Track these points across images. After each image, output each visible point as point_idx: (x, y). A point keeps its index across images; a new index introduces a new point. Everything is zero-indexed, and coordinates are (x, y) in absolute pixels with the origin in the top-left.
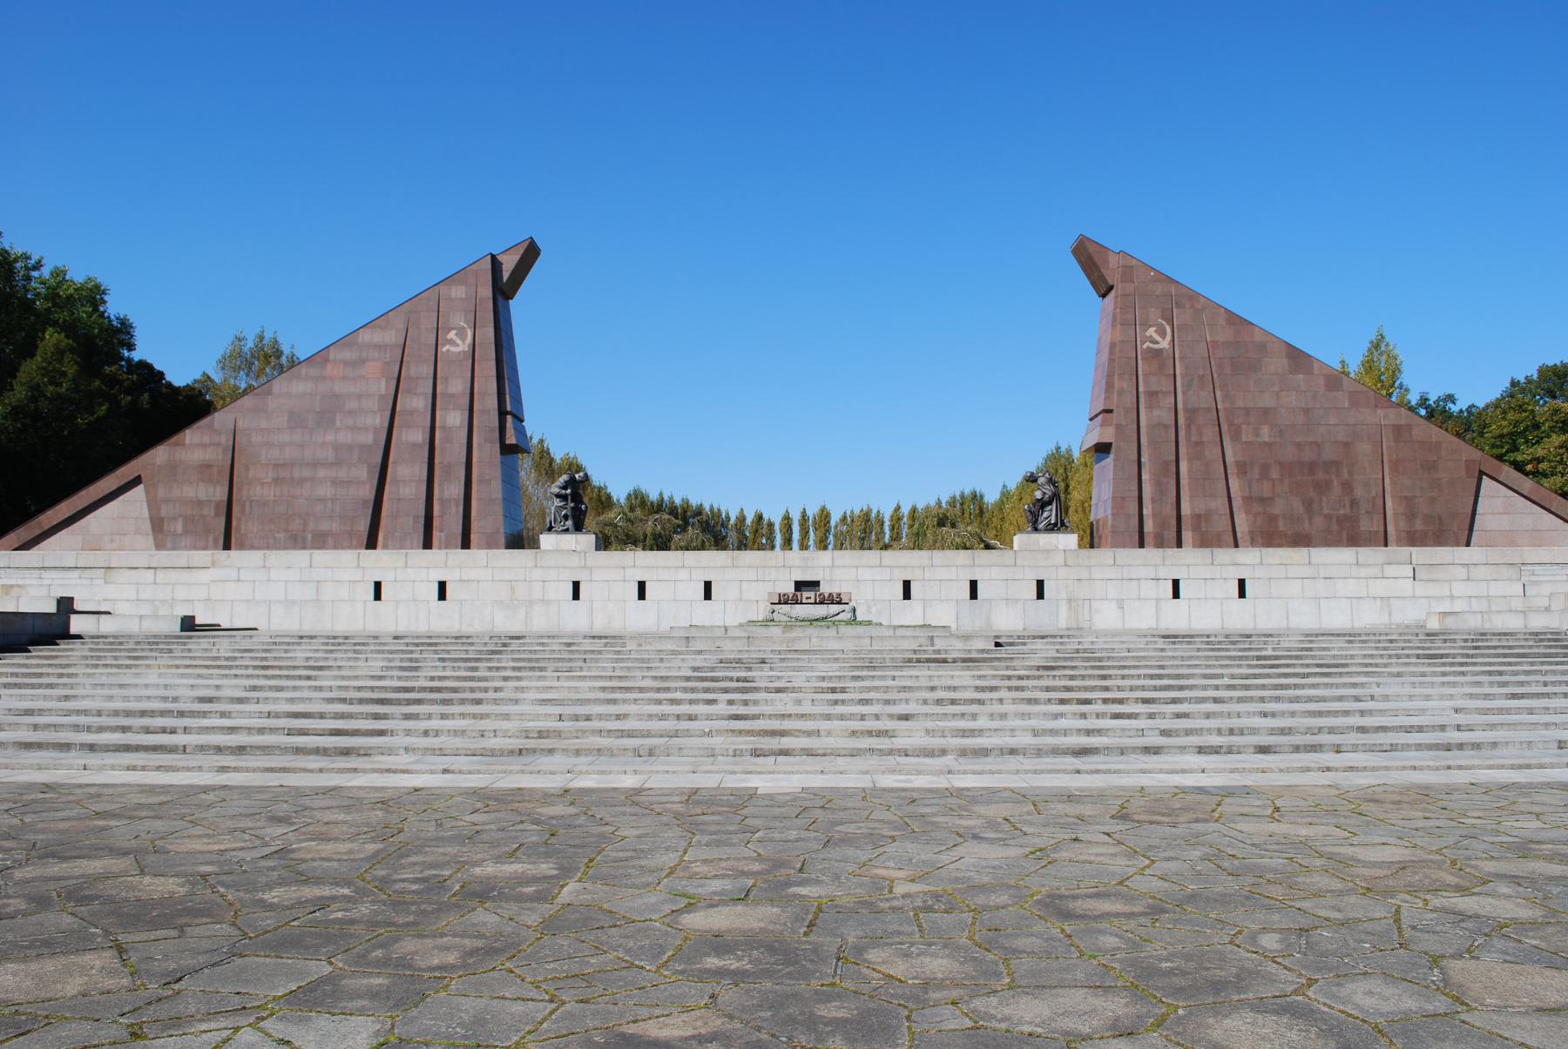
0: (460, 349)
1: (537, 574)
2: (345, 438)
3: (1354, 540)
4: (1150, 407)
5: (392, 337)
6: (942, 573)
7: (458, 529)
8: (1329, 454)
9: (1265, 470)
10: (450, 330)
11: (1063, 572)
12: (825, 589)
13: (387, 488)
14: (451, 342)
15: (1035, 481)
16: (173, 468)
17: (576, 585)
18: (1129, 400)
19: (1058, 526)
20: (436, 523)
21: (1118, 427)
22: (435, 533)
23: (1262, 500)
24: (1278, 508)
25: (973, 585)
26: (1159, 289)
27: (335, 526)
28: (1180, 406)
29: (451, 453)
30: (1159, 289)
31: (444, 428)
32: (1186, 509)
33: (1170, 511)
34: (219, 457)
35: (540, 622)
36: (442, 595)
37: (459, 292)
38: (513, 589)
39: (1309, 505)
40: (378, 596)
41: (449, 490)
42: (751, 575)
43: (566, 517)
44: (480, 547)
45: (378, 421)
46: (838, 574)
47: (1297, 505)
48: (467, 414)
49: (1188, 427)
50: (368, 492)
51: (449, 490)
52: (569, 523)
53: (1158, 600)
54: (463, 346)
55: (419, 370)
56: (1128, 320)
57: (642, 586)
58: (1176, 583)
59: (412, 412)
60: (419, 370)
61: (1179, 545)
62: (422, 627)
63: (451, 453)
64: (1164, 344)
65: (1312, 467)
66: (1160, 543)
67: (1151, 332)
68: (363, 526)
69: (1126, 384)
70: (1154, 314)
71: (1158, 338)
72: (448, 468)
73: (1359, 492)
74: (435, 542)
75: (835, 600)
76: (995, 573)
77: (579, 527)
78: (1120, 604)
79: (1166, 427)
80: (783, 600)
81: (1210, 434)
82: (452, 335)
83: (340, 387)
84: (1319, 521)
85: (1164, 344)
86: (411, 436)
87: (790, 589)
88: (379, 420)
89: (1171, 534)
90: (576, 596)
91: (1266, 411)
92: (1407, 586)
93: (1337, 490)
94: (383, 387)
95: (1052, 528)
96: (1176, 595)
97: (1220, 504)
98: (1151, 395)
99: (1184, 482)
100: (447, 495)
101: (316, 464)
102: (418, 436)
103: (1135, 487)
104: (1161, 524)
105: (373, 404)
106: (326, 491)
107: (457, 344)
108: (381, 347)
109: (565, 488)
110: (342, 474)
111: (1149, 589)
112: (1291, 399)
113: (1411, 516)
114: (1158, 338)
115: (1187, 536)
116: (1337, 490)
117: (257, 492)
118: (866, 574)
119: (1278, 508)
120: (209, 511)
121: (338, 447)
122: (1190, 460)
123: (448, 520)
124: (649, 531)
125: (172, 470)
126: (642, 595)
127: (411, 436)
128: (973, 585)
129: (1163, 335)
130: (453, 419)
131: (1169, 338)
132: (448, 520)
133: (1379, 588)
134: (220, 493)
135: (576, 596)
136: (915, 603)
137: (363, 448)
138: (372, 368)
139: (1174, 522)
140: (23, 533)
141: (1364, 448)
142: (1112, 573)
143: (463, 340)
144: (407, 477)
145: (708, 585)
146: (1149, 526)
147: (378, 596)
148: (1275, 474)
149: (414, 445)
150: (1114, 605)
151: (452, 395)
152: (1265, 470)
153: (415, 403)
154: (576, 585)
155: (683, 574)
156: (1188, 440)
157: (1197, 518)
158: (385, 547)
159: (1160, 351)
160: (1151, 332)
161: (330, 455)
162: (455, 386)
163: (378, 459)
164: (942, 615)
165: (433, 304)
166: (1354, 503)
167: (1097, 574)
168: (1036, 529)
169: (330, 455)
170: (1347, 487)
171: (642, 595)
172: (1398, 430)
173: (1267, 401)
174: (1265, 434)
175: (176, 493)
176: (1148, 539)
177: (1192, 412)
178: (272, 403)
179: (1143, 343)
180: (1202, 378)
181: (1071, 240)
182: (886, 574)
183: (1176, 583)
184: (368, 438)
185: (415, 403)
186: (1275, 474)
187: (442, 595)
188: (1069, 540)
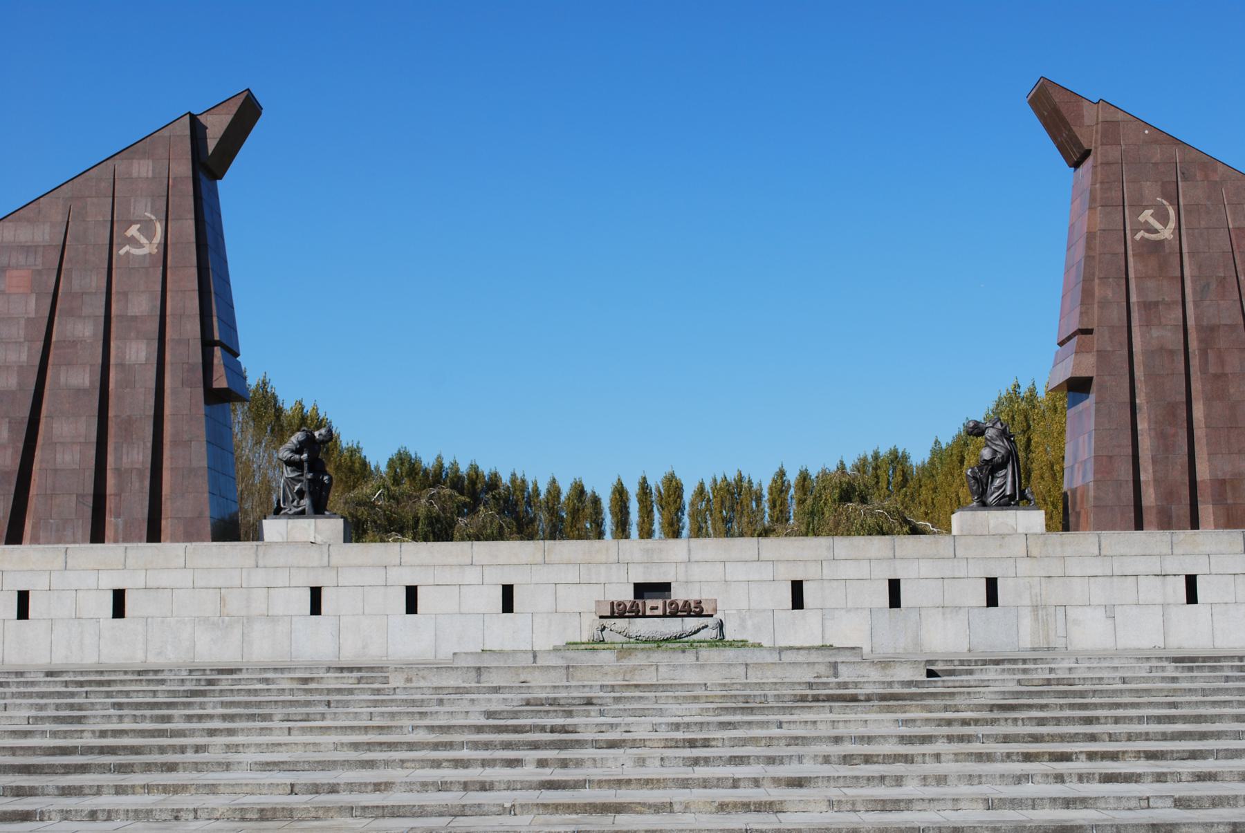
0: (145, 251)
1: (259, 578)
4: (1147, 324)
5: (44, 234)
6: (849, 570)
7: (142, 511)
10: (131, 223)
11: (1025, 567)
12: (679, 594)
13: (38, 453)
14: (133, 241)
15: (982, 433)
17: (316, 593)
18: (1116, 315)
20: (110, 504)
21: (1102, 355)
22: (110, 520)
25: (894, 587)
26: (1157, 154)
28: (1191, 322)
29: (132, 402)
30: (1157, 154)
31: (121, 365)
32: (1203, 472)
33: (1179, 475)
35: (262, 648)
36: (119, 610)
37: (143, 168)
38: (222, 599)
40: (23, 613)
41: (130, 456)
42: (572, 576)
43: (301, 494)
44: (174, 539)
45: (24, 357)
46: (697, 572)
48: (155, 345)
49: (1204, 353)
51: (130, 456)
52: (306, 502)
53: (1164, 606)
54: (149, 247)
55: (85, 281)
56: (1112, 200)
57: (412, 593)
58: (1191, 581)
59: (74, 343)
60: (85, 281)
61: (1195, 524)
62: (89, 658)
63: (132, 402)
66: (1166, 523)
67: (1147, 216)
69: (1108, 292)
70: (1150, 189)
71: (1158, 226)
72: (128, 425)
74: (109, 531)
75: (694, 610)
76: (926, 568)
77: (319, 509)
78: (1110, 611)
79: (1172, 353)
80: (618, 612)
82: (133, 231)
86: (73, 377)
87: (628, 595)
88: (27, 356)
89: (1184, 509)
90: (316, 609)
94: (32, 307)
95: (1006, 503)
96: (1192, 598)
98: (1149, 307)
99: (1199, 433)
100: (126, 462)
102: (83, 378)
103: (1128, 441)
104: (1168, 495)
105: (17, 331)
107: (141, 244)
108: (28, 249)
109: (298, 451)
111: (1151, 590)
114: (1158, 226)
115: (1206, 511)
118: (738, 572)
122: (1208, 400)
123: (128, 500)
124: (422, 512)
126: (412, 607)
127: (73, 377)
128: (894, 587)
129: (1164, 220)
130: (135, 352)
131: (1172, 224)
132: (128, 500)
135: (316, 609)
139: (1186, 492)
142: (1096, 567)
143: (150, 237)
145: (508, 591)
146: (1149, 497)
147: (23, 613)
149: (79, 392)
150: (1100, 613)
151: (134, 318)
153: (80, 329)
154: (316, 593)
155: (472, 576)
156: (1204, 370)
157: (1221, 485)
158: (35, 540)
159: (1160, 244)
160: (1147, 216)
162: (138, 304)
163: (25, 412)
164: (849, 631)
165: (106, 186)
167: (1075, 568)
168: (984, 505)
171: (412, 607)
176: (1148, 517)
177: (1209, 332)
179: (1135, 231)
180: (1222, 281)
181: (1028, 86)
182: (766, 572)
183: (1191, 581)
184: (12, 382)
185: (80, 329)
187: (119, 610)
188: (1032, 520)
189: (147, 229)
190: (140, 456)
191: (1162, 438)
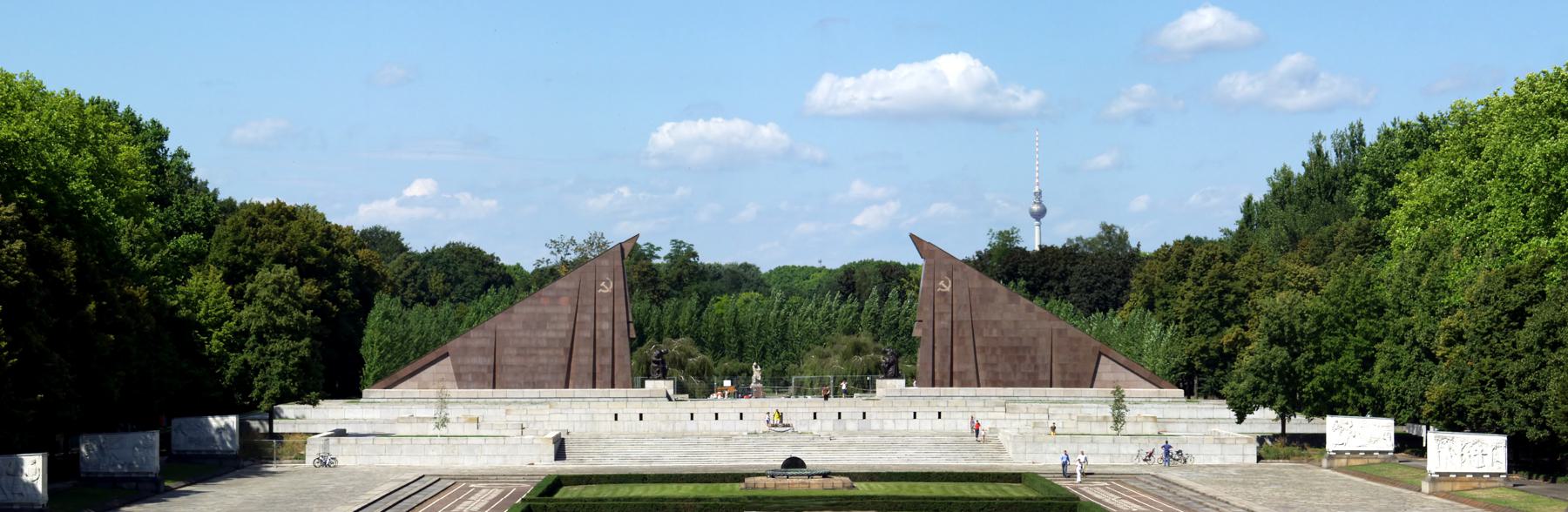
2: (552, 334)
3: (1035, 384)
8: (1025, 343)
9: (994, 350)
16: (466, 349)
19: (896, 376)
23: (993, 365)
24: (999, 369)
26: (947, 262)
27: (549, 377)
29: (604, 342)
30: (947, 262)
32: (955, 369)
33: (947, 370)
34: (488, 343)
37: (605, 262)
39: (1014, 367)
47: (1008, 367)
50: (564, 361)
54: (608, 290)
64: (948, 289)
65: (1017, 349)
66: (942, 385)
68: (562, 377)
70: (943, 273)
73: (1039, 361)
77: (664, 377)
81: (968, 333)
83: (549, 310)
84: (1019, 376)
85: (948, 289)
88: (567, 326)
91: (995, 323)
92: (1002, 415)
93: (1028, 361)
94: (568, 310)
97: (972, 366)
98: (941, 314)
101: (538, 348)
102: (588, 334)
104: (943, 376)
106: (544, 360)
110: (551, 352)
111: (904, 415)
112: (1009, 316)
113: (1064, 373)
116: (1028, 361)
117: (510, 361)
119: (999, 369)
120: (485, 370)
121: (548, 339)
125: (466, 349)
130: (606, 326)
133: (992, 415)
134: (490, 361)
136: (818, 422)
137: (562, 340)
138: (564, 300)
140: (388, 381)
141: (1043, 341)
144: (583, 357)
146: (937, 377)
148: (999, 352)
152: (994, 350)
161: (544, 343)
162: (607, 310)
166: (1036, 367)
169: (544, 343)
170: (1033, 359)
172: (1060, 332)
173: (996, 317)
174: (995, 333)
175: (468, 361)
177: (960, 323)
178: (514, 317)
184: (563, 335)
186: (999, 352)
189: (607, 283)
190: (608, 360)
191: (943, 359)
